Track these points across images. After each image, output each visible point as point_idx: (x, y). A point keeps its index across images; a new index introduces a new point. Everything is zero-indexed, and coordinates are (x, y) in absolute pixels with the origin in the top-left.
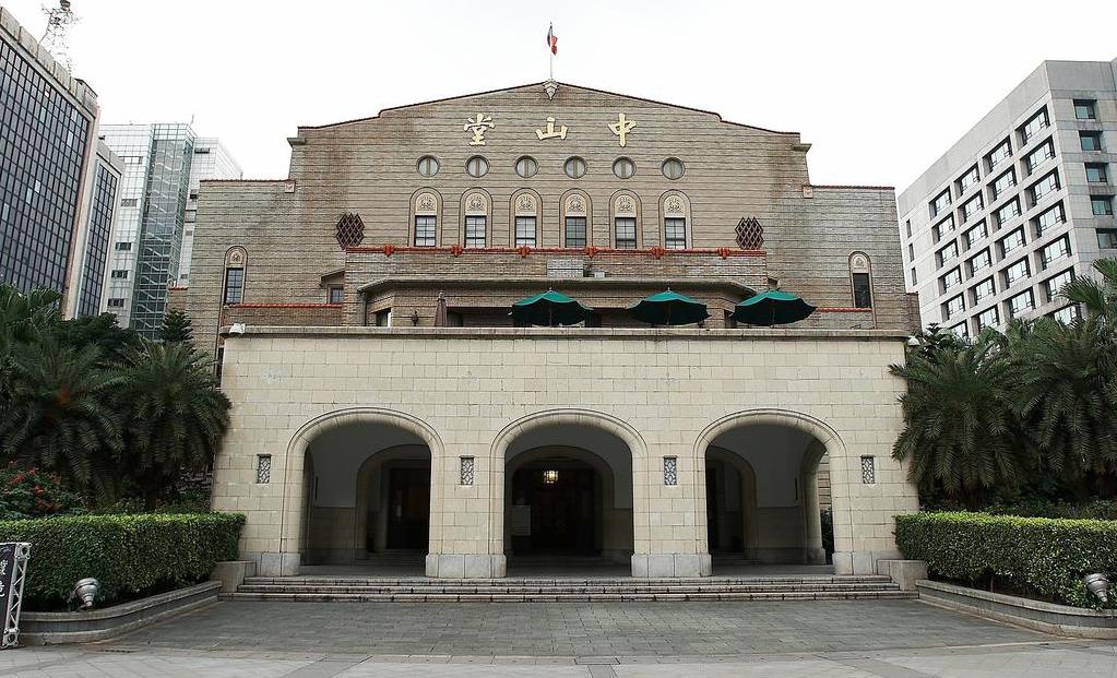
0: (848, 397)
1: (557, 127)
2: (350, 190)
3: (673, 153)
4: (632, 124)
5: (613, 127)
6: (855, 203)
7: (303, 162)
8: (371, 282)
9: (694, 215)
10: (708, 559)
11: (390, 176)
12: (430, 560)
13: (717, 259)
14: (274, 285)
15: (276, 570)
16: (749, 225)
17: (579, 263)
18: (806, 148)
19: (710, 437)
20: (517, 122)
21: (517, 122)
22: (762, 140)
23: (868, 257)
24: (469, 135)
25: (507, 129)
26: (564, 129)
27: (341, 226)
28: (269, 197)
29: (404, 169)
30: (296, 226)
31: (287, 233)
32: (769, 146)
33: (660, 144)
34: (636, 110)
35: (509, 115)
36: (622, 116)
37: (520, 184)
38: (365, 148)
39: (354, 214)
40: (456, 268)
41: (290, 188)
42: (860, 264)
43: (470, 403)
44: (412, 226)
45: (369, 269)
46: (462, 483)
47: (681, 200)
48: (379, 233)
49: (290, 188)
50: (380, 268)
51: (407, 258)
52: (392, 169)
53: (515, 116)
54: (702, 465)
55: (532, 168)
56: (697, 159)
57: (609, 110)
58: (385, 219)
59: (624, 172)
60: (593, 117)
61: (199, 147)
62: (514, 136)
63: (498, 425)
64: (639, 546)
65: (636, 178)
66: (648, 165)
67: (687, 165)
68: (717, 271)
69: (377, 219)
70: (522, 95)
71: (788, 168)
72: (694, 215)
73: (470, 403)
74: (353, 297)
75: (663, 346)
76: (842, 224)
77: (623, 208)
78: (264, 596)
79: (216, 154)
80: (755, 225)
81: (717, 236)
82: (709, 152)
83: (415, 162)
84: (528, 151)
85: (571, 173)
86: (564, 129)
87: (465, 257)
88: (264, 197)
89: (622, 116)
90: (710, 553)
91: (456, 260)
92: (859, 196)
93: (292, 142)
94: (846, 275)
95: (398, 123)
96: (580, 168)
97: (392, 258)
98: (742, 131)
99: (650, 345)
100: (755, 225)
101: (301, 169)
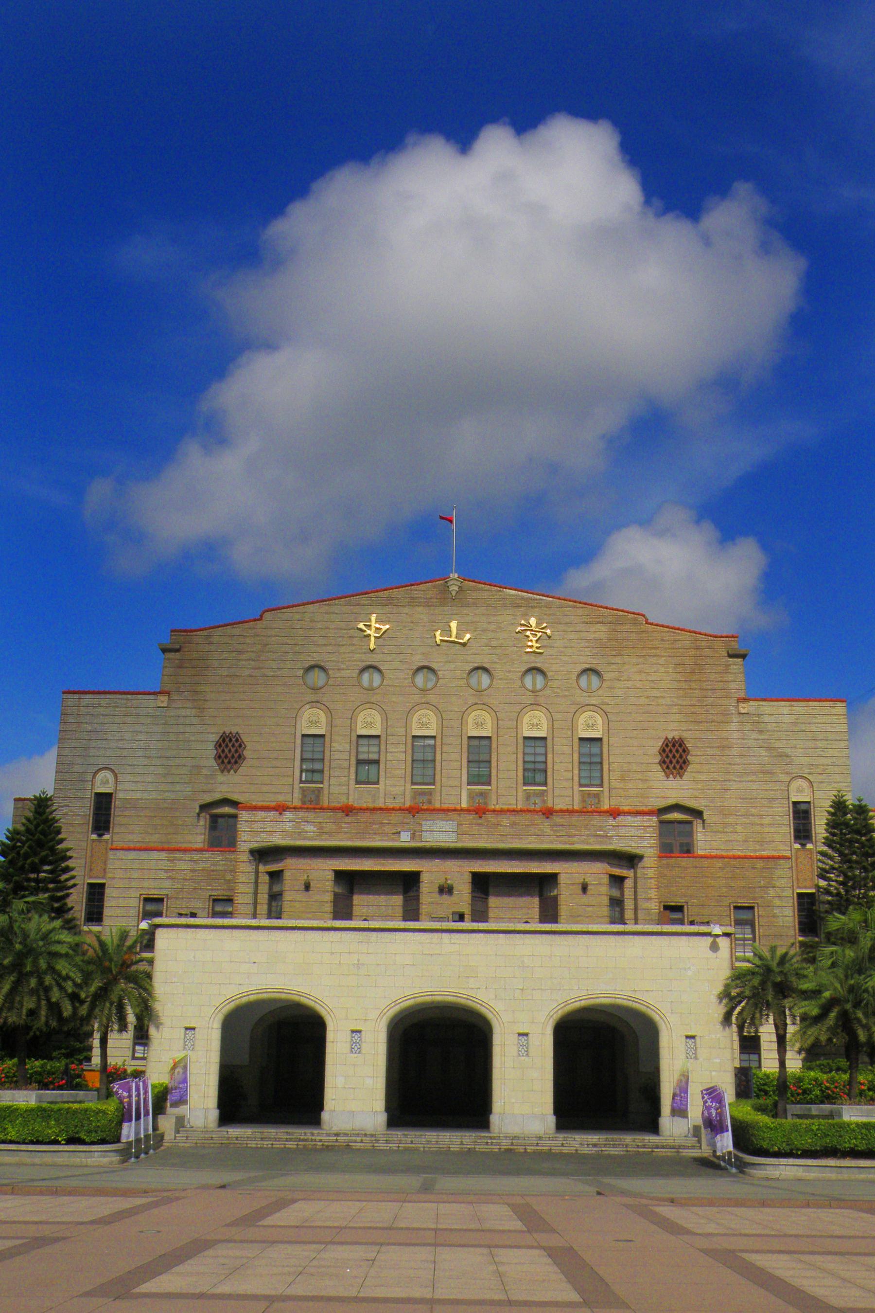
0: (678, 982)
16: (674, 745)
27: (220, 746)
39: (234, 731)
46: (352, 1052)
59: (534, 684)
67: (606, 676)
73: (360, 982)
74: (245, 857)
80: (680, 745)
96: (485, 680)
100: (680, 745)
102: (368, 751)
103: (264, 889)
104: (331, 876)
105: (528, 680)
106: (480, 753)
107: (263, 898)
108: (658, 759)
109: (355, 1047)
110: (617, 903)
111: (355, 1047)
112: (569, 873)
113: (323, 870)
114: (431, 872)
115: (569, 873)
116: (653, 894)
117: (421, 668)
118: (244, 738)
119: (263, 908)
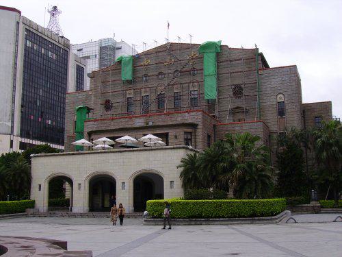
8: (91, 130)
13: (186, 114)
15: (42, 211)
41: (90, 93)
45: (90, 126)
49: (90, 93)
51: (99, 122)
61: (117, 46)
76: (271, 84)
78: (37, 215)
99: (120, 154)
115: (172, 133)
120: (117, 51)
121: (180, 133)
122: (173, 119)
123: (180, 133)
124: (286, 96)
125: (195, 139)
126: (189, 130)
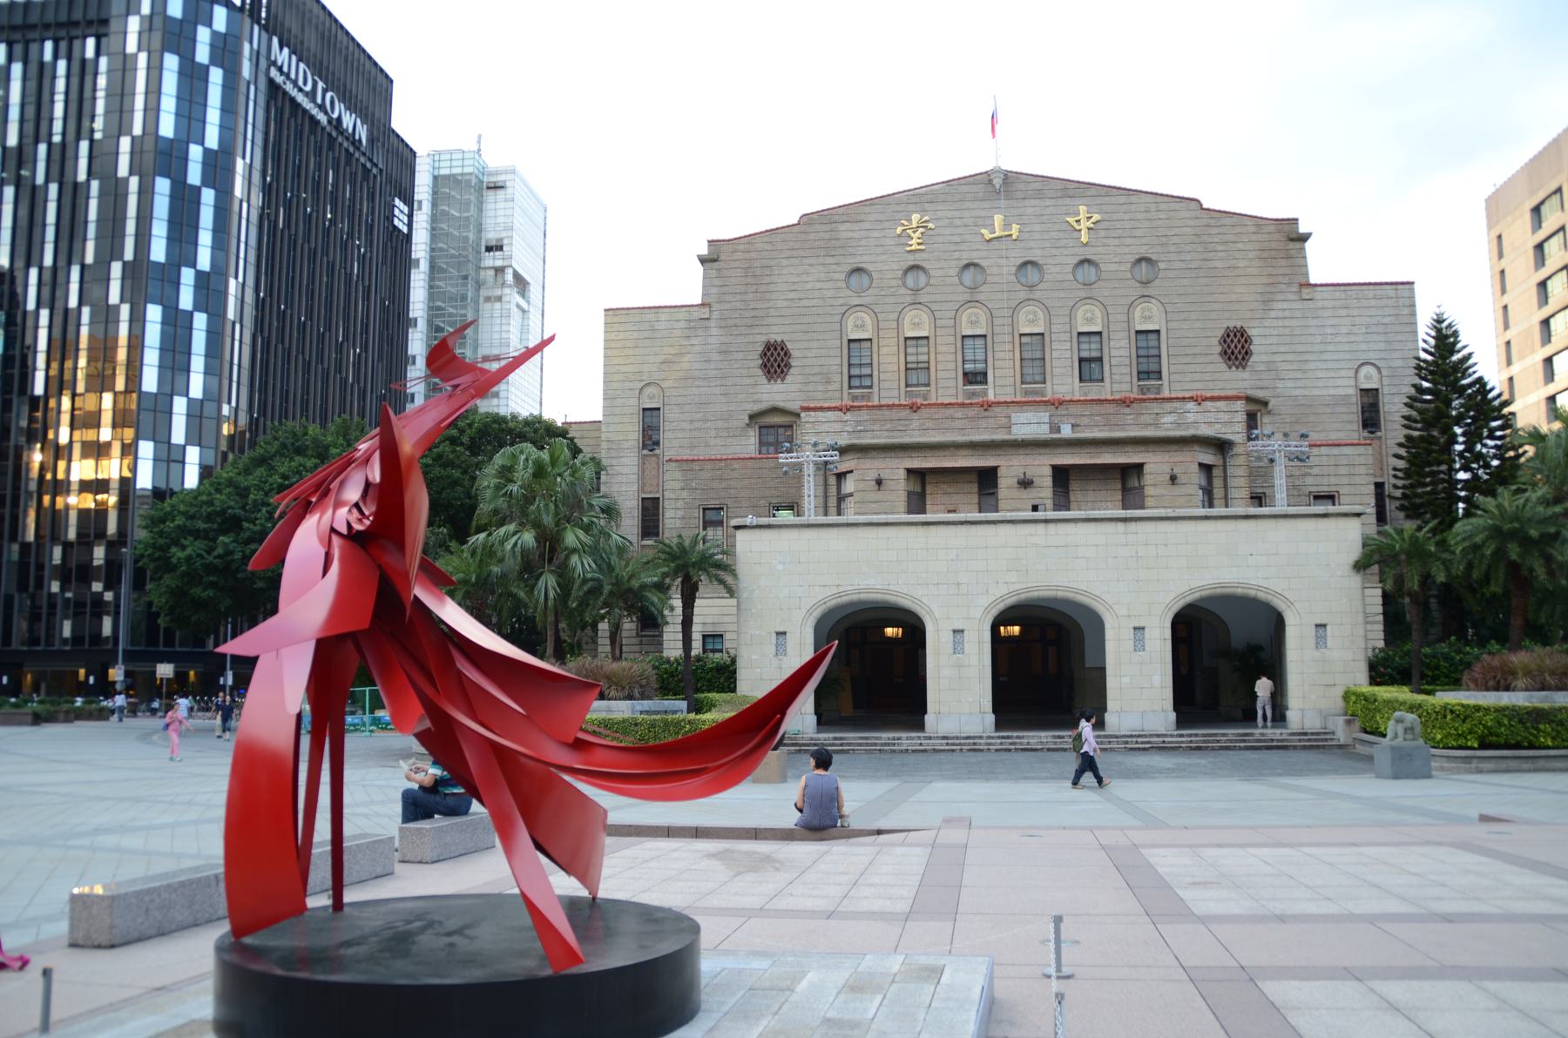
1: (1007, 225)
2: (772, 312)
3: (1144, 251)
4: (1096, 217)
5: (1071, 220)
6: (1364, 303)
7: (717, 282)
9: (1172, 325)
10: (1172, 716)
11: (816, 294)
12: (929, 719)
13: (1191, 405)
14: (696, 425)
17: (1044, 416)
18: (1304, 238)
19: (1176, 609)
20: (958, 222)
21: (958, 222)
22: (1252, 229)
23: (1378, 369)
24: (903, 240)
25: (948, 231)
26: (1015, 227)
28: (682, 324)
29: (830, 285)
30: (716, 357)
31: (705, 366)
32: (1260, 237)
33: (1129, 241)
34: (1099, 200)
35: (950, 214)
36: (1082, 209)
37: (967, 297)
38: (785, 262)
39: (779, 340)
40: (915, 424)
41: (705, 313)
42: (1368, 377)
43: (956, 580)
44: (845, 351)
45: (825, 427)
47: (1154, 307)
48: (806, 361)
49: (705, 313)
50: (837, 427)
52: (818, 285)
53: (957, 214)
54: (1168, 634)
55: (979, 278)
56: (1173, 257)
57: (1067, 201)
58: (814, 345)
60: (1049, 211)
62: (957, 239)
63: (985, 601)
64: (1110, 704)
65: (1101, 284)
66: (1113, 267)
67: (1162, 265)
68: (1191, 417)
69: (805, 345)
70: (965, 189)
71: (1284, 262)
72: (1172, 325)
75: (1133, 526)
77: (1089, 321)
79: (515, 188)
81: (1197, 350)
82: (1188, 248)
83: (843, 276)
84: (975, 257)
85: (1023, 280)
86: (1015, 227)
87: (924, 412)
88: (676, 325)
89: (1082, 209)
90: (1176, 709)
91: (915, 416)
92: (1371, 294)
93: (703, 260)
94: (1352, 391)
95: (822, 230)
96: (1032, 275)
97: (849, 416)
98: (1228, 221)
99: (1120, 526)
101: (714, 290)
102: (918, 354)
103: (833, 490)
104: (902, 474)
105: (1080, 274)
106: (1034, 351)
107: (833, 502)
108: (1218, 349)
109: (958, 647)
110: (1208, 492)
111: (958, 647)
112: (1156, 465)
113: (895, 469)
114: (1010, 468)
116: (1242, 482)
117: (967, 266)
118: (789, 346)
119: (833, 510)
120: (490, 196)
121: (1188, 463)
122: (1143, 419)
123: (1188, 463)
124: (1385, 372)
125: (1226, 487)
126: (1208, 458)
